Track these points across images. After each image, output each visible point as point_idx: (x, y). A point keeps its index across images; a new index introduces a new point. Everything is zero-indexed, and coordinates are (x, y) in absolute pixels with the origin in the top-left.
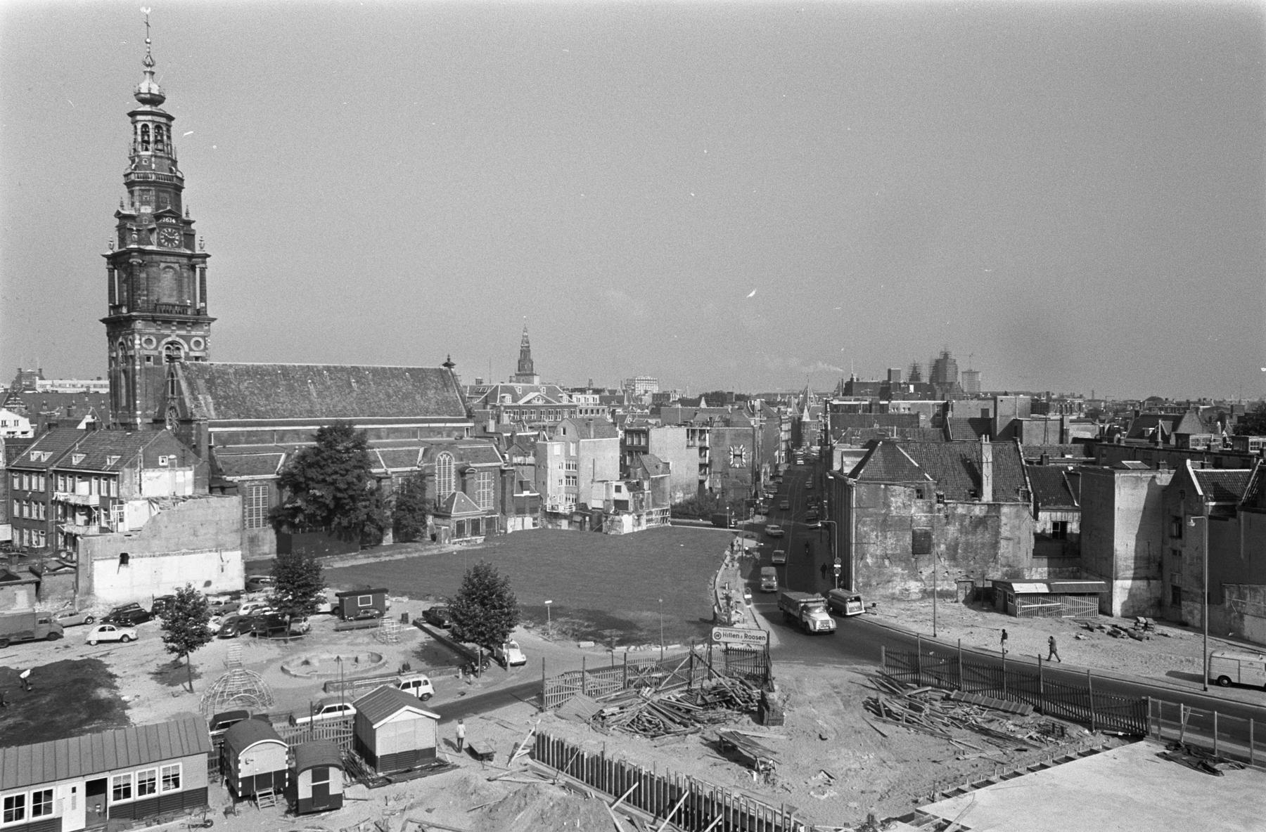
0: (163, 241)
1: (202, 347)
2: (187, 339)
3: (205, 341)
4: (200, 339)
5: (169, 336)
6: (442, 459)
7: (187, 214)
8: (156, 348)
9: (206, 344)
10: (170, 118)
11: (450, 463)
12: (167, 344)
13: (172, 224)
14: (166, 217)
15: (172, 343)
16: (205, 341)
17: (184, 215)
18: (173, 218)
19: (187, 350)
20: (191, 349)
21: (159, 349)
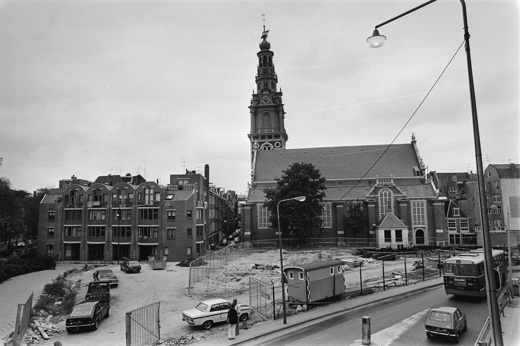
0: (263, 102)
1: (279, 146)
2: (273, 143)
5: (265, 142)
6: (383, 193)
7: (281, 90)
9: (281, 144)
10: (272, 53)
11: (390, 195)
12: (264, 146)
13: (267, 94)
14: (264, 91)
15: (267, 145)
17: (278, 91)
18: (267, 91)
19: (273, 148)
20: (274, 147)
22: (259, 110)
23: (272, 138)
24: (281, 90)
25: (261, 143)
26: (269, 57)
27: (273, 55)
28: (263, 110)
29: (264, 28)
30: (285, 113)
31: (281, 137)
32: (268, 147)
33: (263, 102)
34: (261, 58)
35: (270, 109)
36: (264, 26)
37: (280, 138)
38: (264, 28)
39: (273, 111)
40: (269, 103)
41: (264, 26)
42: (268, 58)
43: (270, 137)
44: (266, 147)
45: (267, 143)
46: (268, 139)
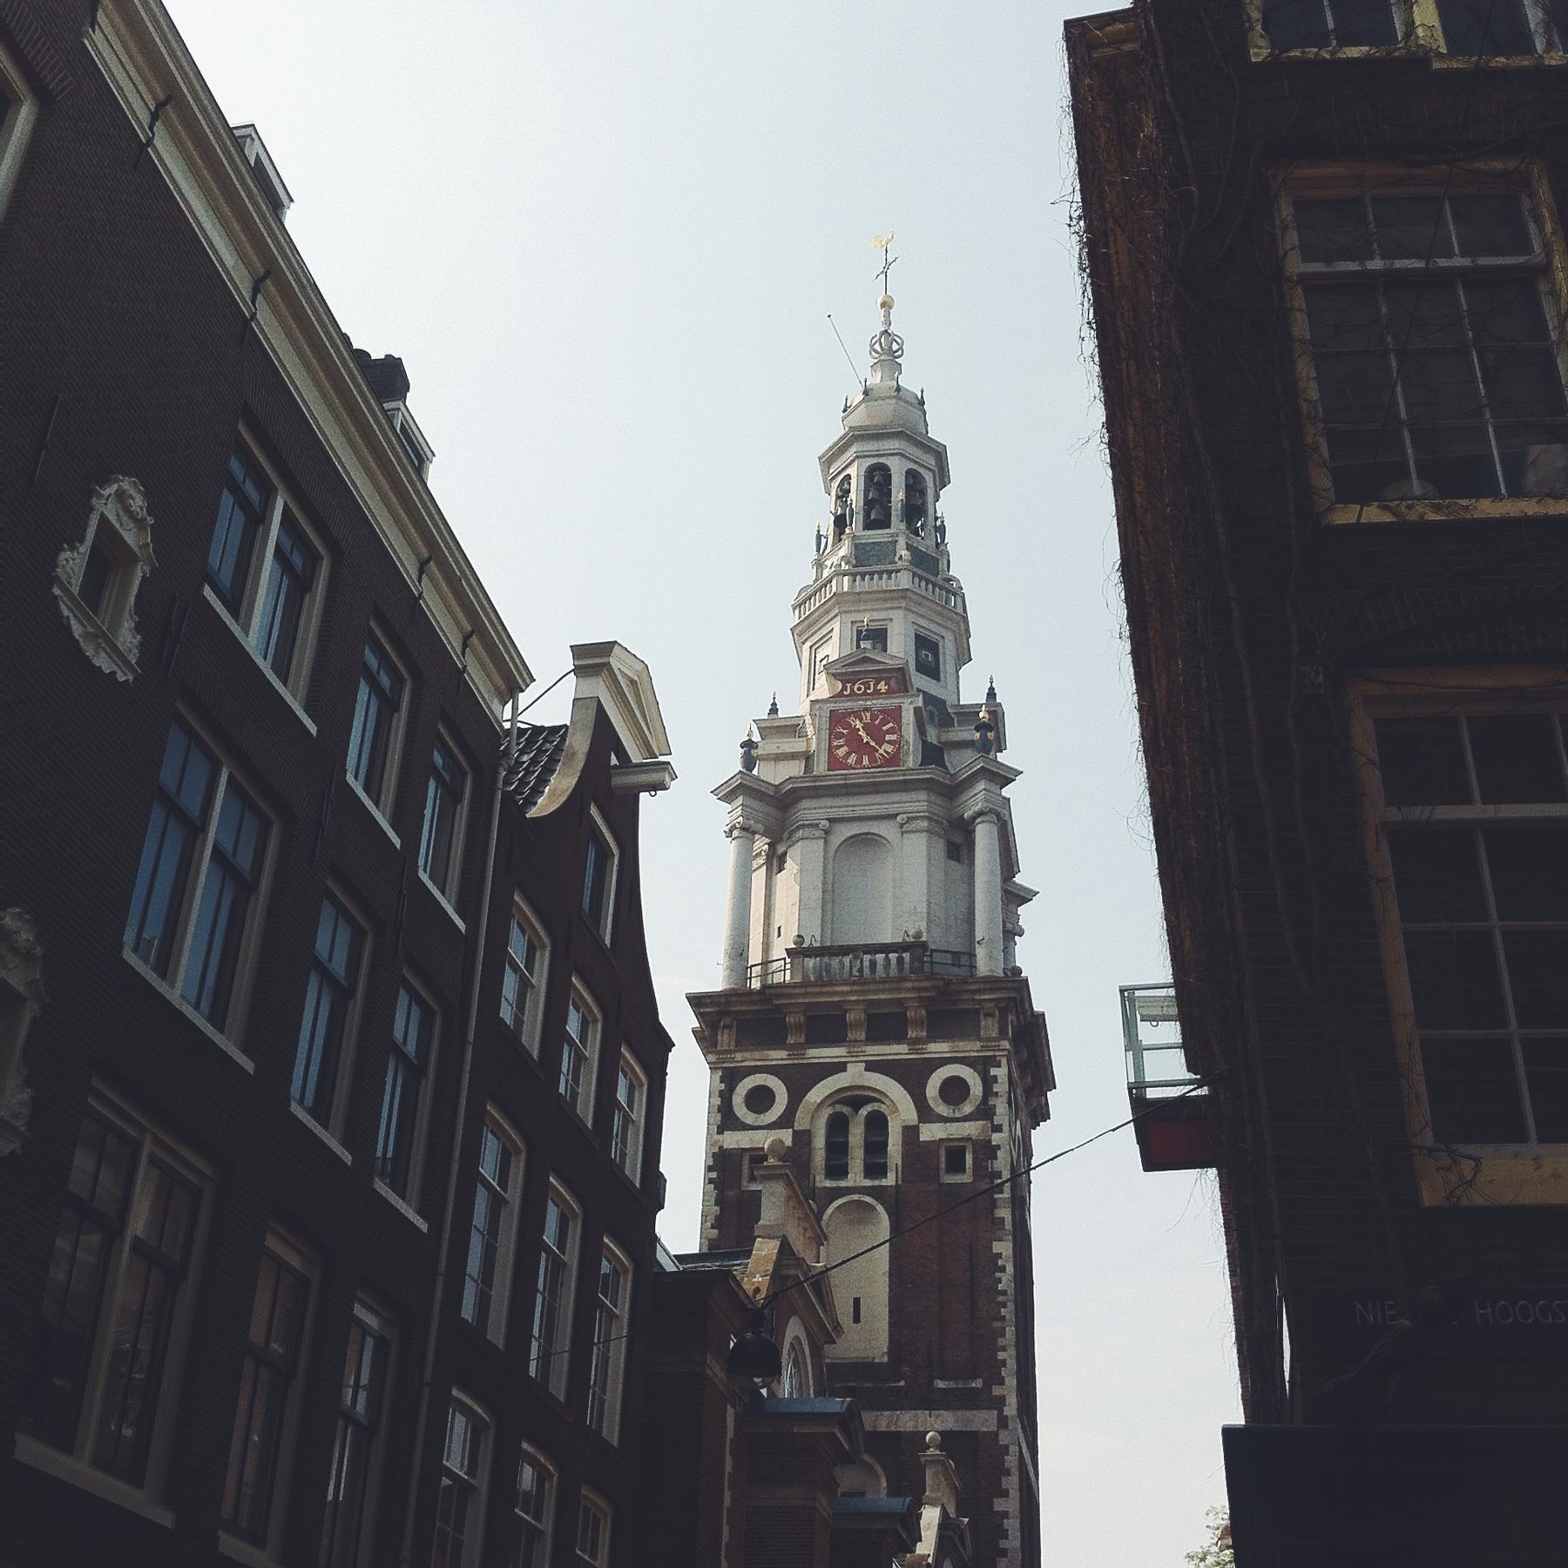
0: (841, 752)
2: (911, 1076)
3: (988, 1082)
4: (965, 1072)
5: (841, 1067)
8: (785, 1121)
10: (939, 454)
15: (855, 1098)
16: (988, 1082)
20: (926, 1114)
21: (801, 1121)
22: (811, 810)
23: (900, 1038)
24: (992, 694)
25: (800, 1079)
27: (943, 479)
28: (834, 813)
29: (888, 315)
30: (1024, 896)
31: (989, 1027)
32: (864, 1112)
33: (841, 752)
34: (849, 476)
35: (892, 810)
36: (887, 305)
37: (973, 1033)
38: (888, 315)
39: (925, 824)
40: (894, 759)
41: (887, 305)
43: (883, 1026)
44: (839, 1108)
45: (855, 1075)
46: (872, 1039)
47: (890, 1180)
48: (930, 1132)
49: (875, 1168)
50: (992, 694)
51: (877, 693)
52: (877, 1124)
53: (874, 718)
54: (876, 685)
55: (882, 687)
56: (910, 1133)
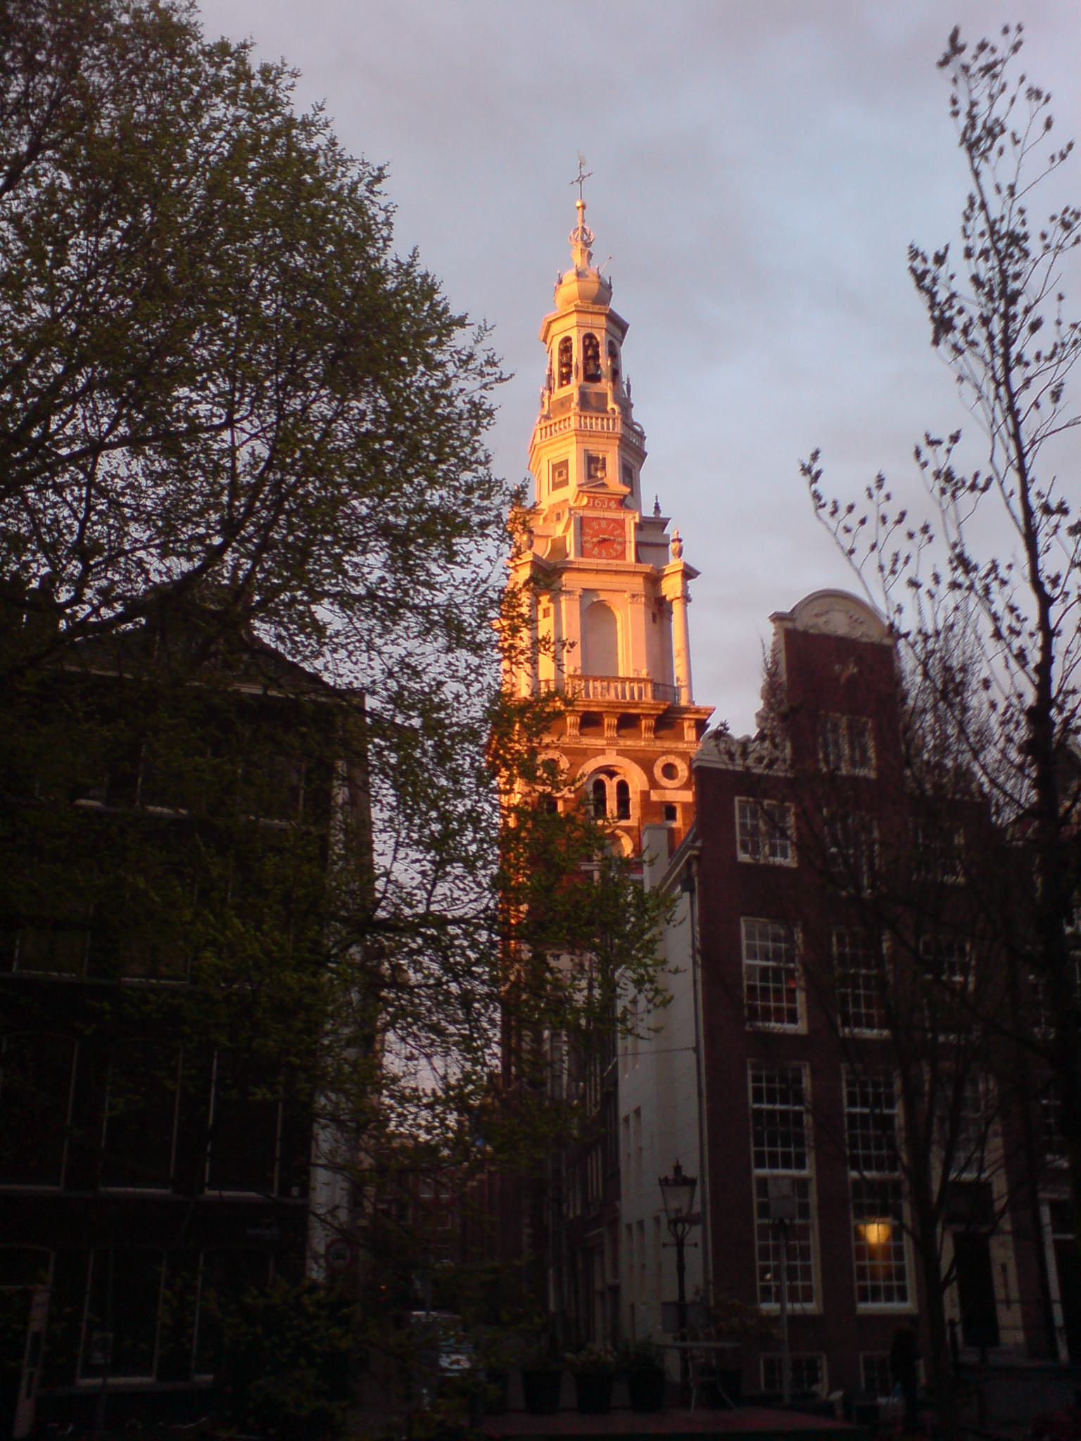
5: (602, 752)
20: (654, 784)
24: (657, 508)
26: (611, 344)
34: (568, 339)
42: (603, 350)
44: (603, 777)
45: (610, 759)
47: (632, 822)
48: (655, 796)
49: (624, 812)
50: (657, 508)
51: (609, 508)
52: (623, 788)
53: (608, 525)
54: (610, 500)
55: (613, 504)
56: (645, 795)
